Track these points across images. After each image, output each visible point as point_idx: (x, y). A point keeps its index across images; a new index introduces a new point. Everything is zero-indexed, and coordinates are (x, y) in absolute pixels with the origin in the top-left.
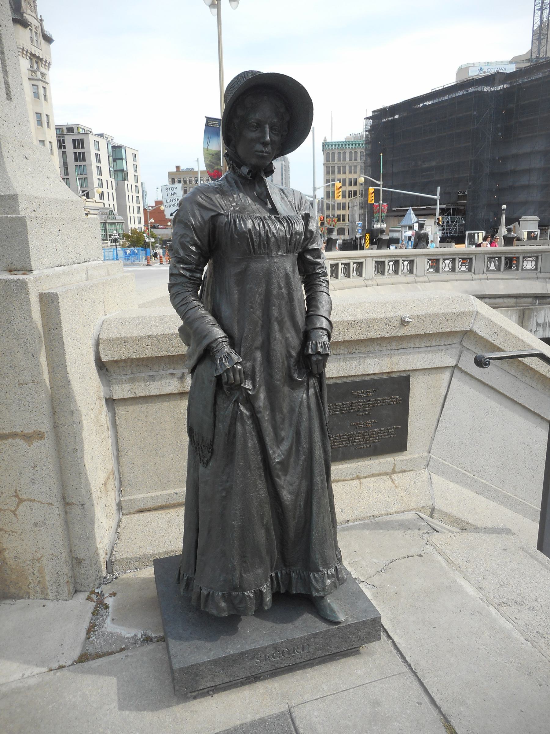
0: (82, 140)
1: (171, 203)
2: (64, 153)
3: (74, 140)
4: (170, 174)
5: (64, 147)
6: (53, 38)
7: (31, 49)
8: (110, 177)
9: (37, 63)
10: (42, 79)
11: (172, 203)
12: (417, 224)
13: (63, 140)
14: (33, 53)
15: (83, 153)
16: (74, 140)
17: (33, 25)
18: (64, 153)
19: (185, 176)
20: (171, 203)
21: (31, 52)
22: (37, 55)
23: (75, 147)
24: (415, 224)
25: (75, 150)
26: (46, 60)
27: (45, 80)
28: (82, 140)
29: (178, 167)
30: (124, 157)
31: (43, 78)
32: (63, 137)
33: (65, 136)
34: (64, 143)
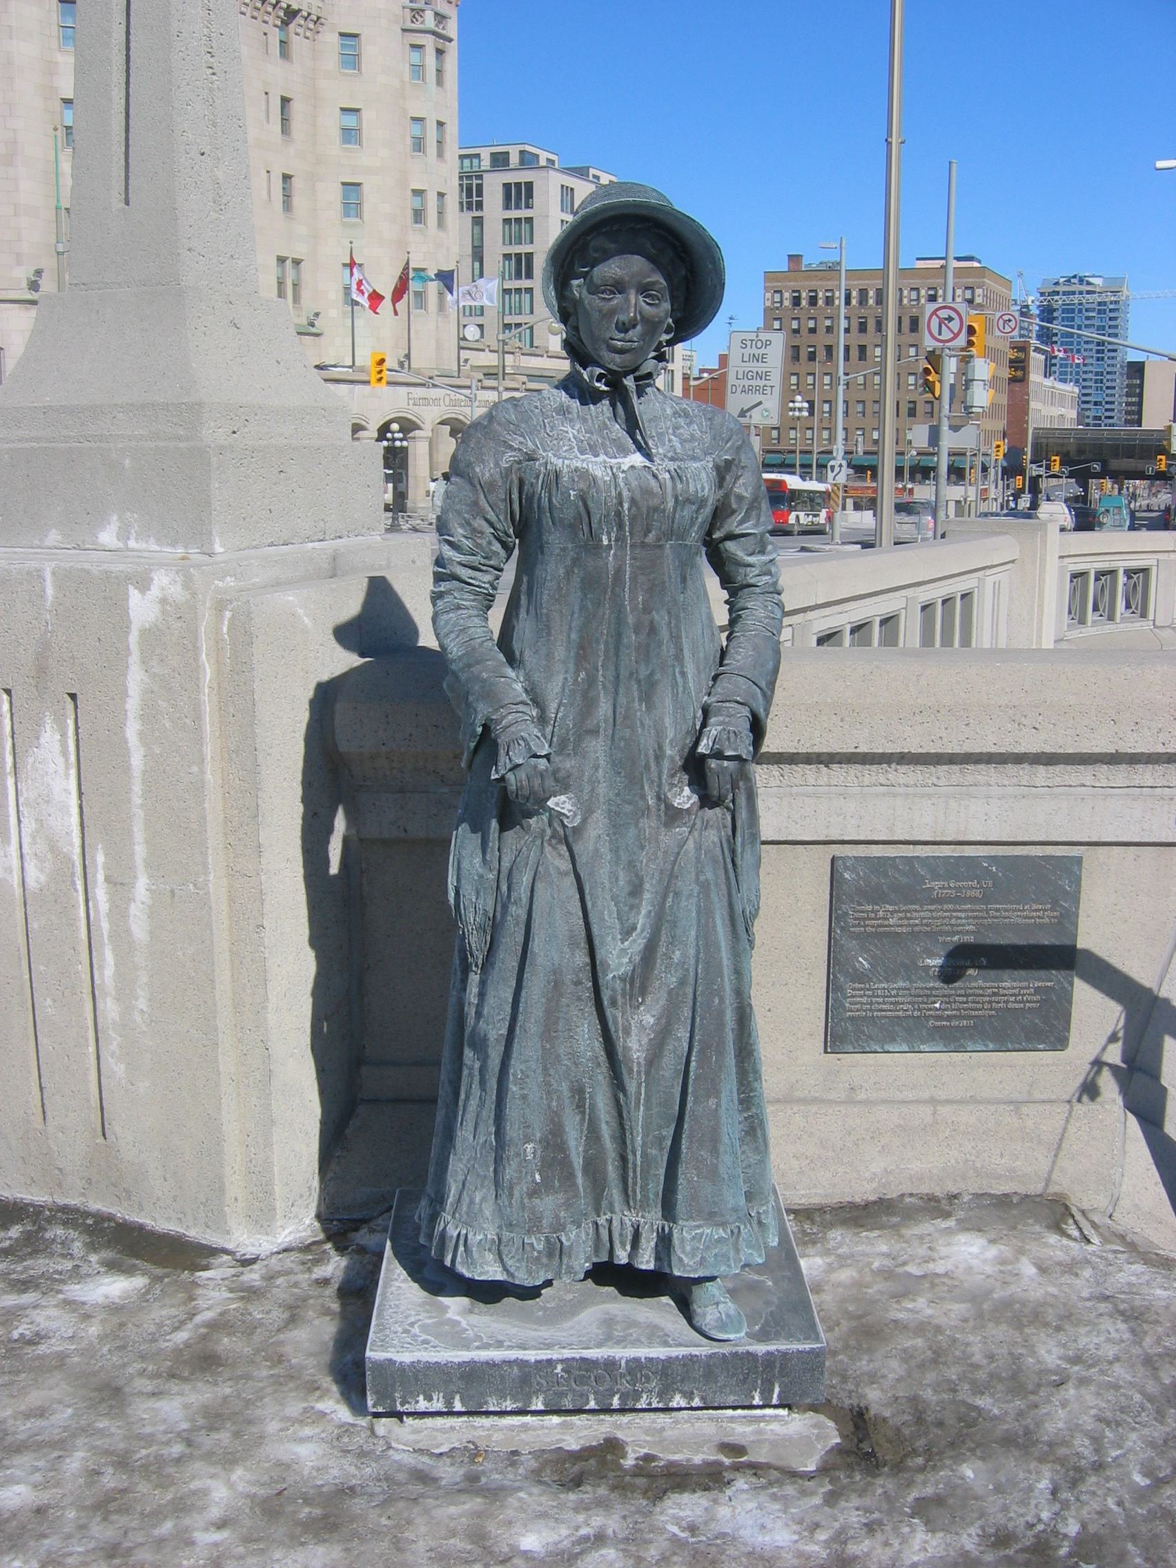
1: (746, 383)
2: (478, 221)
3: (507, 187)
4: (769, 276)
5: (480, 205)
10: (436, 29)
11: (751, 382)
13: (480, 188)
15: (529, 220)
16: (507, 187)
18: (478, 221)
19: (814, 284)
20: (746, 383)
23: (507, 206)
27: (444, 32)
28: (529, 186)
29: (794, 259)
32: (480, 177)
33: (485, 176)
34: (480, 194)
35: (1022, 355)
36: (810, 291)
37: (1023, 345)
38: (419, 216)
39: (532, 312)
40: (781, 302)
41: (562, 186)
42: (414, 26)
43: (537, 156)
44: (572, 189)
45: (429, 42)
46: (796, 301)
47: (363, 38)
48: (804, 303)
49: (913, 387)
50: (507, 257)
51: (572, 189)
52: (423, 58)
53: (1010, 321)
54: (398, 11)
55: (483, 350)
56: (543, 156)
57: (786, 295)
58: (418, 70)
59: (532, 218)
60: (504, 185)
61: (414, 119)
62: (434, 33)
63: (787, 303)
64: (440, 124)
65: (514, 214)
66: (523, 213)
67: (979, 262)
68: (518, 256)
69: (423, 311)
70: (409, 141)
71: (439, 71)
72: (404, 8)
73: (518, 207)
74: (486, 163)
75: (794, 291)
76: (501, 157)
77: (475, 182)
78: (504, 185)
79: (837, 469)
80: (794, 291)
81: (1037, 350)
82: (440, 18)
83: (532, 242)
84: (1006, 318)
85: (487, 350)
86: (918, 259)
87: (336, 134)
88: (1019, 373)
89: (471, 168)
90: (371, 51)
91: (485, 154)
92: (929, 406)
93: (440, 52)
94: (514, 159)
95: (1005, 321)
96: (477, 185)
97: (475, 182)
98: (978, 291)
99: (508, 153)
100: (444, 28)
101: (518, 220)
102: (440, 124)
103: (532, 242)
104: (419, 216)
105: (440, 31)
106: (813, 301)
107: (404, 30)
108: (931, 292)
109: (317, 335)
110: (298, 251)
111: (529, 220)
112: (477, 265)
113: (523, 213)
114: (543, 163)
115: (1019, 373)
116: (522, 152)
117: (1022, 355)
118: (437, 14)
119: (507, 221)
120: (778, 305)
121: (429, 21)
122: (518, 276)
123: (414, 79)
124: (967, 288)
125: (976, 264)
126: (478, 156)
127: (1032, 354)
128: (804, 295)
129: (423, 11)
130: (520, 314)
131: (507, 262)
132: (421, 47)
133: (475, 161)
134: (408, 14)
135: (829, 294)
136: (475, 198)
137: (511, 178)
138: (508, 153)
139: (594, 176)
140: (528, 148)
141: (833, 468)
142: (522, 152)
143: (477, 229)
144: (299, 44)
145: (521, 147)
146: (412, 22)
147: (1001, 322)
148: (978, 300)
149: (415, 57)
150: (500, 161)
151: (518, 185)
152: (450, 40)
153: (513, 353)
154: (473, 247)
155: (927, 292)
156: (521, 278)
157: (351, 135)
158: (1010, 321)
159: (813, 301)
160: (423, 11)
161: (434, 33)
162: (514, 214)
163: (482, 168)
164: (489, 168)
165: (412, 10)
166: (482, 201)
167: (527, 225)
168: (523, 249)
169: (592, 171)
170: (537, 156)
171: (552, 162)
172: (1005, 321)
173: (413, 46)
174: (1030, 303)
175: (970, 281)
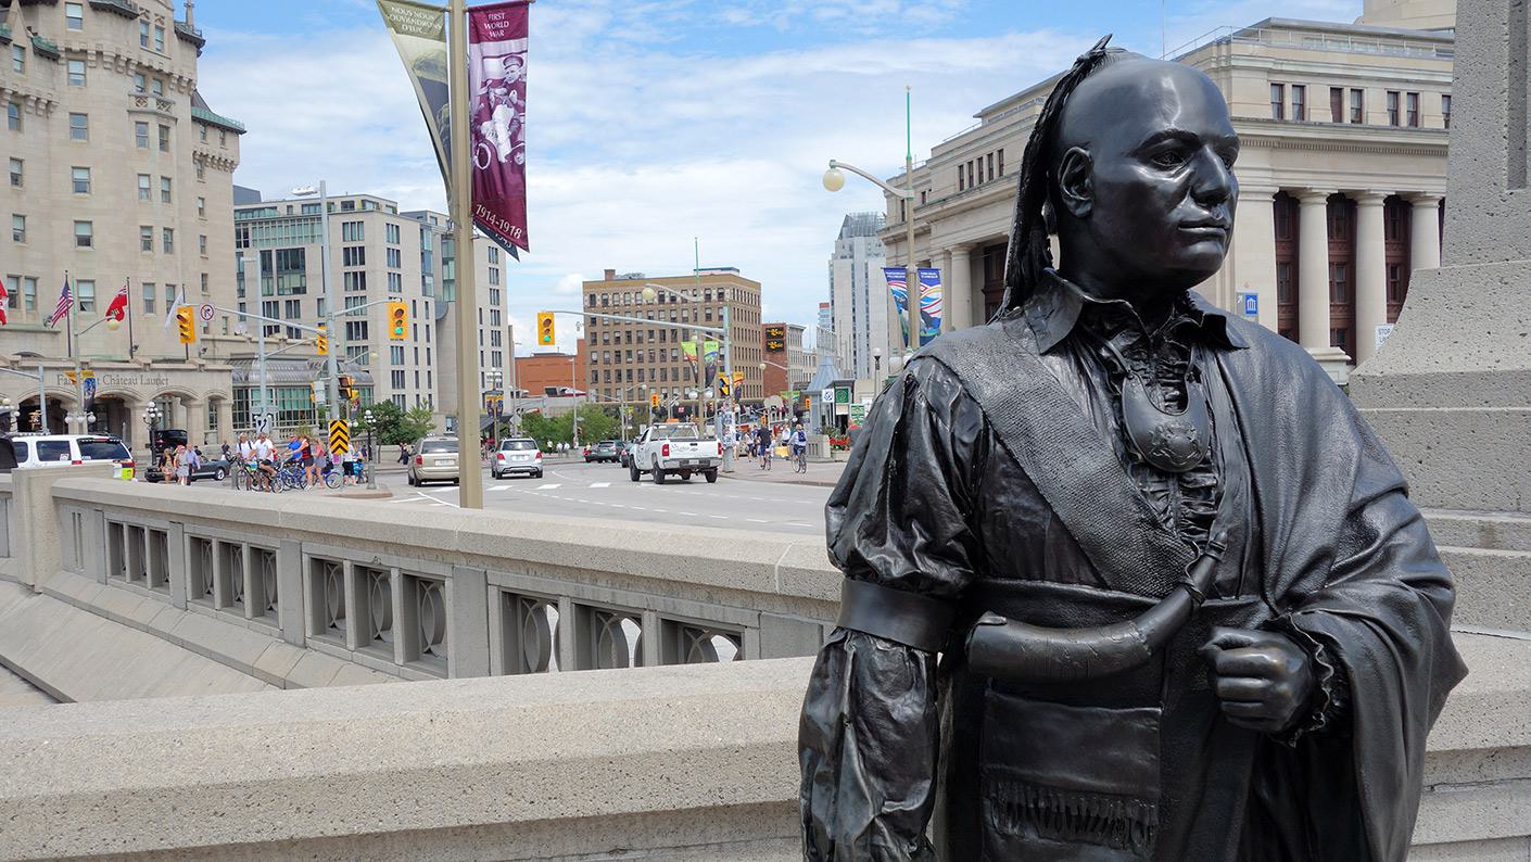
6: (204, 38)
7: (140, 56)
8: (424, 295)
10: (159, 111)
14: (146, 63)
17: (151, 15)
21: (140, 63)
22: (156, 67)
26: (181, 77)
38: (147, 245)
42: (138, 109)
44: (397, 227)
47: (89, 116)
51: (397, 227)
58: (142, 139)
62: (155, 113)
68: (355, 274)
71: (164, 144)
79: (263, 424)
82: (163, 103)
84: (206, 308)
87: (70, 187)
90: (96, 126)
93: (164, 129)
104: (147, 245)
105: (163, 111)
109: (56, 333)
110: (32, 271)
118: (159, 101)
121: (152, 104)
122: (356, 288)
137: (348, 218)
141: (260, 422)
144: (29, 121)
157: (81, 187)
161: (155, 113)
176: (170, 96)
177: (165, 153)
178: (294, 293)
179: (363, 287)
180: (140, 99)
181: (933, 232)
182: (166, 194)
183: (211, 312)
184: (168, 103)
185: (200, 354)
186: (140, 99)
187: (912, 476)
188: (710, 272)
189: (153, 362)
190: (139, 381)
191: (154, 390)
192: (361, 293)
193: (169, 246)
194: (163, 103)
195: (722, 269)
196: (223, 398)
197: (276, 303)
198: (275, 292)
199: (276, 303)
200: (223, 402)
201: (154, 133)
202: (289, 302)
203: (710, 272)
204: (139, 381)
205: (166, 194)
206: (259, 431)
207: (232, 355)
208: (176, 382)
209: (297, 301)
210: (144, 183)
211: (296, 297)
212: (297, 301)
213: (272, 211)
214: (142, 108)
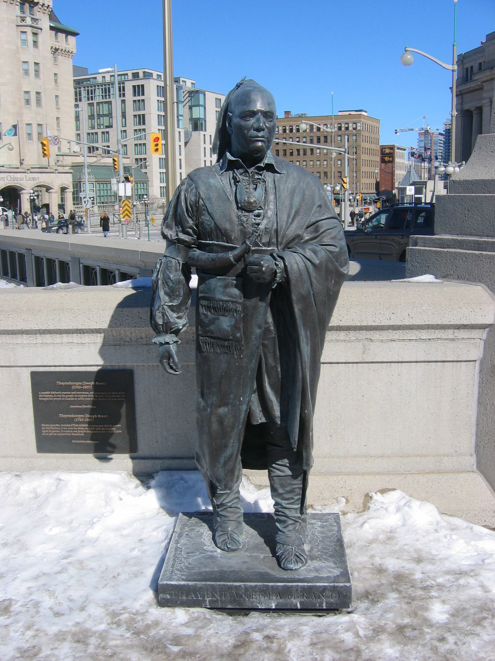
0: (143, 86)
2: (123, 102)
3: (134, 87)
5: (124, 95)
9: (31, 8)
10: (32, 24)
12: (413, 188)
13: (124, 87)
15: (143, 101)
16: (134, 87)
18: (123, 102)
19: (291, 123)
23: (135, 95)
24: (408, 188)
25: (135, 97)
26: (44, 4)
28: (143, 86)
30: (202, 103)
31: (35, 24)
32: (123, 83)
33: (126, 83)
34: (124, 90)
35: (392, 151)
36: (290, 126)
37: (392, 147)
38: (28, 102)
39: (145, 139)
40: (278, 131)
41: (158, 86)
42: (22, 24)
43: (152, 74)
45: (29, 30)
46: (285, 131)
48: (294, 131)
49: (312, 166)
50: (135, 116)
52: (27, 36)
53: (57, 139)
54: (14, 18)
55: (79, 156)
56: (155, 74)
57: (280, 128)
58: (24, 42)
59: (144, 100)
60: (133, 86)
61: (24, 62)
62: (31, 26)
63: (281, 132)
64: (36, 64)
65: (137, 98)
66: (141, 98)
67: (366, 112)
68: (139, 115)
69: (31, 141)
70: (21, 71)
71: (35, 43)
72: (17, 16)
73: (139, 95)
74: (130, 77)
75: (283, 127)
76: (136, 75)
77: (122, 85)
78: (133, 86)
79: (87, 202)
80: (283, 127)
81: (398, 148)
82: (34, 20)
83: (144, 110)
84: (55, 138)
85: (81, 156)
86: (339, 111)
88: (391, 159)
89: (121, 79)
91: (130, 74)
92: (340, 174)
93: (35, 34)
94: (141, 75)
95: (55, 139)
96: (123, 86)
97: (122, 85)
98: (359, 124)
99: (138, 73)
100: (37, 24)
101: (139, 101)
102: (36, 64)
103: (144, 110)
104: (28, 102)
105: (35, 25)
106: (291, 130)
107: (17, 26)
108: (339, 125)
111: (143, 101)
112: (124, 120)
113: (141, 98)
114: (155, 77)
115: (391, 159)
116: (144, 72)
117: (392, 151)
118: (32, 19)
119: (134, 101)
120: (277, 132)
121: (29, 21)
122: (140, 124)
123: (23, 45)
124: (353, 123)
125: (363, 113)
126: (127, 74)
127: (396, 150)
128: (287, 128)
129: (25, 17)
130: (141, 140)
131: (135, 119)
132: (25, 32)
133: (126, 77)
134: (19, 19)
135: (298, 127)
136: (122, 92)
138: (138, 73)
139: (183, 81)
140: (146, 70)
141: (85, 202)
142: (144, 72)
143: (123, 105)
145: (144, 70)
146: (21, 22)
147: (54, 140)
148: (358, 128)
149: (24, 36)
150: (136, 76)
151: (138, 86)
152: (41, 29)
153: (96, 157)
154: (122, 112)
155: (337, 125)
156: (141, 125)
158: (57, 139)
159: (291, 130)
160: (25, 17)
161: (31, 26)
162: (137, 98)
163: (129, 79)
164: (131, 79)
165: (21, 17)
166: (124, 93)
167: (143, 103)
168: (141, 113)
169: (181, 79)
170: (152, 74)
171: (160, 76)
172: (55, 139)
173: (22, 32)
174: (428, 129)
175: (355, 120)
176: (38, 15)
177: (36, 49)
178: (106, 128)
179: (144, 124)
180: (23, 19)
181: (485, 88)
182: (37, 72)
183: (58, 140)
184: (37, 20)
185: (56, 163)
186: (23, 19)
187: (179, 210)
188: (348, 113)
189: (32, 168)
190: (24, 179)
191: (33, 184)
192: (142, 127)
193: (39, 102)
194: (34, 20)
195: (356, 111)
196: (67, 188)
197: (96, 133)
198: (96, 127)
199: (96, 133)
200: (67, 190)
201: (30, 38)
202: (103, 133)
203: (348, 113)
204: (24, 179)
205: (37, 72)
206: (84, 207)
207: (72, 163)
208: (44, 179)
209: (108, 132)
210: (25, 66)
211: (107, 130)
212: (108, 132)
213: (94, 80)
214: (23, 23)
